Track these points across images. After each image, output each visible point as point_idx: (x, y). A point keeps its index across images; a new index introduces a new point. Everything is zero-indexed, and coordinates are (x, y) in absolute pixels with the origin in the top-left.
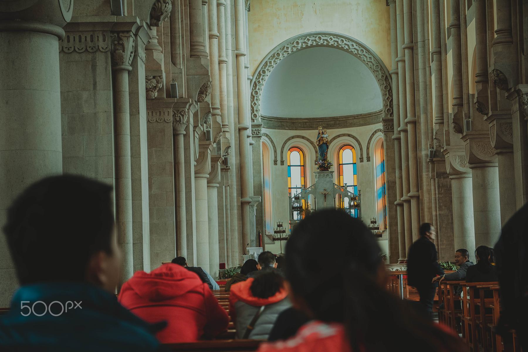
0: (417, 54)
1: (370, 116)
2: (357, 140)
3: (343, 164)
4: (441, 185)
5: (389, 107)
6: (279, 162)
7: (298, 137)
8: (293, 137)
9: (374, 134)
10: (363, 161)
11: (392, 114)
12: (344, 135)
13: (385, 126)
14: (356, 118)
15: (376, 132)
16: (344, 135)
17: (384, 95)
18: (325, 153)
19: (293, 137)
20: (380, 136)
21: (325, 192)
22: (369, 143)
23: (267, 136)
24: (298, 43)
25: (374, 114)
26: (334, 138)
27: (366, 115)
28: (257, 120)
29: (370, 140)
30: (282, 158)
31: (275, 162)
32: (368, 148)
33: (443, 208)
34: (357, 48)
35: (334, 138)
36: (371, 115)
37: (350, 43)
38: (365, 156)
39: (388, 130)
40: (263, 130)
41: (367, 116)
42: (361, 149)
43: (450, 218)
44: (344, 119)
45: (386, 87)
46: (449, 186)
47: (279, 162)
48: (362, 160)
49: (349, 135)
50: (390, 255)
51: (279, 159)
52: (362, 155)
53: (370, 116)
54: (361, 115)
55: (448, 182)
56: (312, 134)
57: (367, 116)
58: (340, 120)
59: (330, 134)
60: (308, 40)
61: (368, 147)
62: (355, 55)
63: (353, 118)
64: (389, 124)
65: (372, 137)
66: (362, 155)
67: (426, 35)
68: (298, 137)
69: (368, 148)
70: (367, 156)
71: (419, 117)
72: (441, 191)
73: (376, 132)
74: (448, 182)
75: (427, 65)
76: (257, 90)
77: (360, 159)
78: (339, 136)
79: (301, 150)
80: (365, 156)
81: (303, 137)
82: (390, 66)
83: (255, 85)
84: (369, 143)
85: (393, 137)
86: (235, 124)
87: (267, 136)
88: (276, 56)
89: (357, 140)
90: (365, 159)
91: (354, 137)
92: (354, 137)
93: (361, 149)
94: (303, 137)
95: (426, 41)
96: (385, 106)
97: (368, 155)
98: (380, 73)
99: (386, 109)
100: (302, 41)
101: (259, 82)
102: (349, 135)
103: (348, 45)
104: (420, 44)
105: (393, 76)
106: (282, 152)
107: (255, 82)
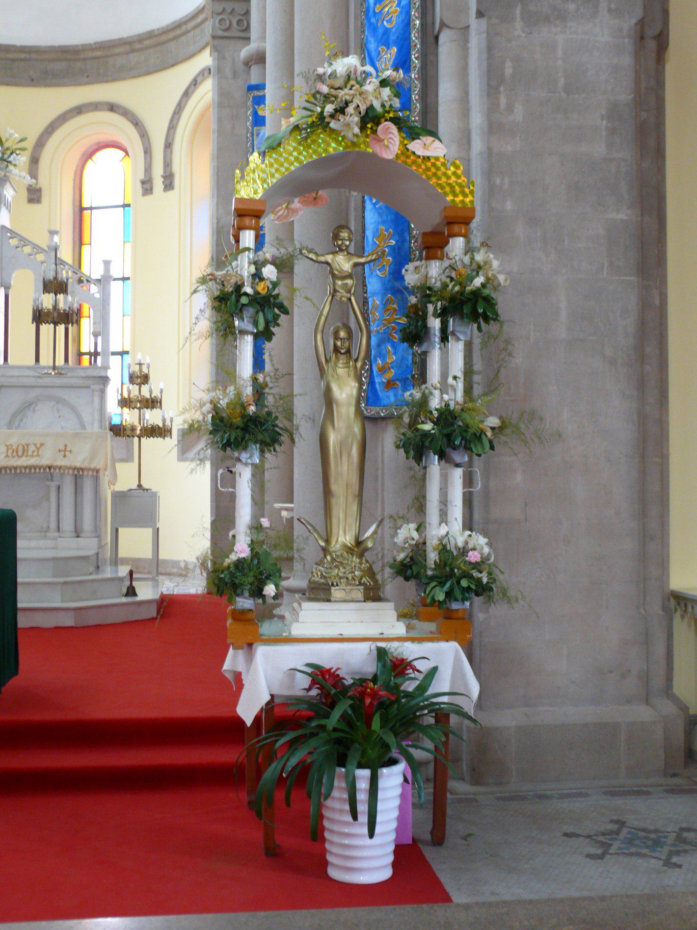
1: (178, 32)
2: (137, 123)
4: (508, 70)
9: (190, 91)
10: (152, 189)
12: (95, 106)
13: (219, 14)
14: (137, 46)
15: (195, 83)
16: (95, 106)
22: (172, 127)
25: (193, 23)
27: (166, 31)
29: (177, 117)
32: (168, 145)
33: (520, 230)
36: (184, 28)
39: (226, 34)
41: (171, 35)
42: (148, 151)
43: (563, 305)
44: (99, 53)
46: (562, 81)
48: (147, 186)
49: (112, 108)
50: (213, 519)
52: (148, 169)
53: (178, 32)
54: (150, 35)
55: (560, 53)
57: (171, 35)
58: (84, 59)
61: (170, 141)
63: (128, 48)
64: (233, 10)
65: (182, 106)
66: (148, 169)
69: (168, 145)
70: (165, 171)
72: (510, 108)
73: (195, 83)
74: (560, 53)
77: (143, 182)
78: (79, 110)
84: (172, 127)
89: (137, 123)
90: (158, 183)
91: (126, 113)
92: (126, 113)
93: (148, 151)
97: (168, 169)
102: (112, 108)
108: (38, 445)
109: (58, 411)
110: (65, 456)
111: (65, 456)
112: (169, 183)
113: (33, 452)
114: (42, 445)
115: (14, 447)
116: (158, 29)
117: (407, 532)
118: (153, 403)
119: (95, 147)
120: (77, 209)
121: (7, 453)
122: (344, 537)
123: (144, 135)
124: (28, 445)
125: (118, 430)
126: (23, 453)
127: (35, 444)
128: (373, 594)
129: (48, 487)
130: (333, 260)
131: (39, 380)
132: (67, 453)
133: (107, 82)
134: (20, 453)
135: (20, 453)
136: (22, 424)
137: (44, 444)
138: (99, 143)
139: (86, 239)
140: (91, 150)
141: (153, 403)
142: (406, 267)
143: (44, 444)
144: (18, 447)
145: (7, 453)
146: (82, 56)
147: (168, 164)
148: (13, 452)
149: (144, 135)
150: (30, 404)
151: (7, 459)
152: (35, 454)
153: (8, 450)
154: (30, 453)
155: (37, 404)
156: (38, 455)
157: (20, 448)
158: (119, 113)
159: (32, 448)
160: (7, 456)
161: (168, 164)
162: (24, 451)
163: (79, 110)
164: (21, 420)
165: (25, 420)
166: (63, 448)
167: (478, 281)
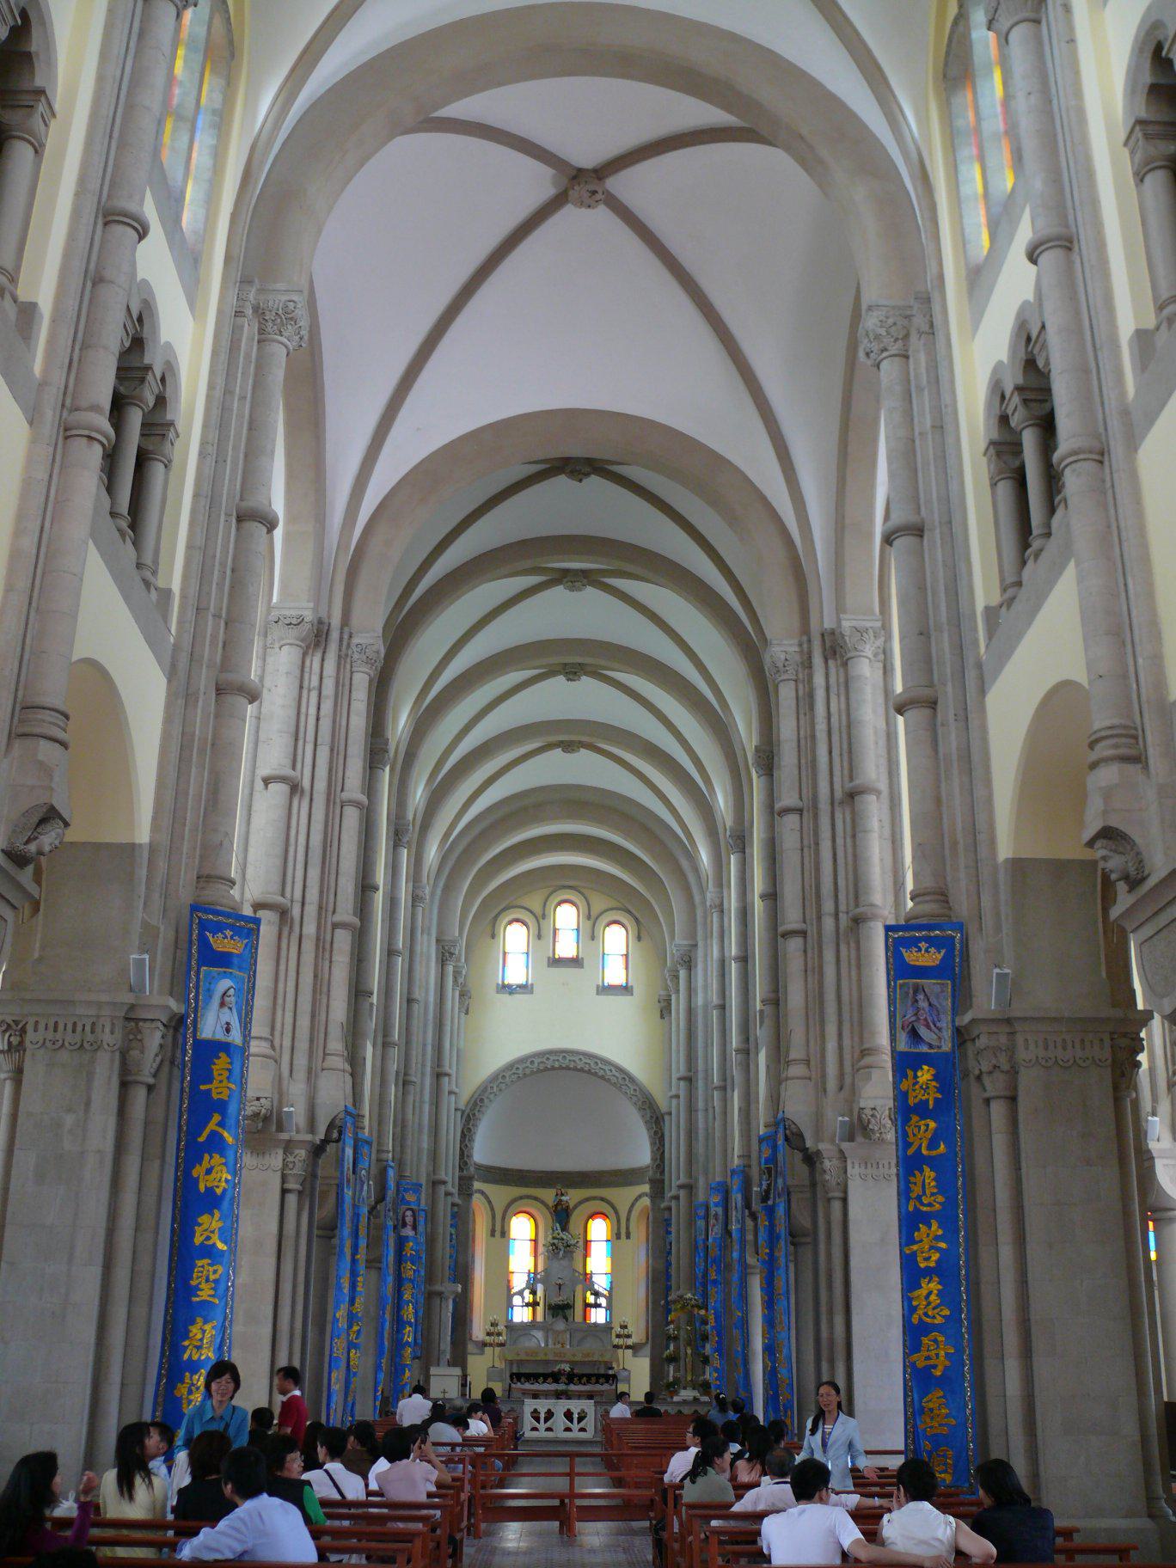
0: (697, 1088)
2: (613, 1207)
5: (658, 1162)
6: (498, 1234)
7: (528, 1197)
8: (521, 1198)
11: (663, 1172)
12: (595, 1198)
15: (640, 1197)
16: (595, 1198)
17: (653, 1144)
19: (521, 1198)
20: (646, 1201)
21: (560, 1281)
22: (630, 1211)
23: (482, 1193)
24: (532, 1062)
26: (580, 1203)
28: (468, 1169)
30: (503, 1227)
31: (493, 1234)
32: (628, 1220)
34: (617, 1074)
35: (580, 1203)
37: (606, 1068)
38: (623, 1231)
40: (477, 1185)
42: (618, 1221)
45: (656, 1133)
47: (498, 1234)
48: (618, 1236)
49: (602, 1199)
51: (498, 1228)
52: (619, 1229)
54: (620, 1171)
56: (549, 1195)
59: (572, 1196)
60: (548, 1059)
62: (614, 1084)
66: (619, 1229)
67: (710, 1062)
68: (528, 1197)
69: (628, 1220)
71: (697, 1180)
73: (640, 1197)
75: (710, 1105)
76: (470, 1126)
78: (587, 1200)
79: (532, 1216)
80: (623, 1231)
81: (536, 1199)
82: (662, 1103)
83: (468, 1119)
84: (630, 1211)
85: (662, 1206)
86: (428, 1175)
87: (482, 1193)
88: (500, 1080)
89: (613, 1207)
91: (608, 1202)
92: (608, 1202)
93: (618, 1221)
94: (536, 1199)
95: (710, 1071)
96: (654, 1159)
98: (648, 1111)
100: (540, 1060)
101: (474, 1115)
102: (602, 1199)
103: (604, 1070)
104: (701, 1075)
105: (666, 1117)
106: (503, 1218)
107: (469, 1115)
112: (628, 1237)
117: (702, 1378)
118: (629, 1336)
122: (689, 1378)
123: (617, 1213)
125: (617, 1347)
128: (694, 1389)
141: (629, 1336)
147: (628, 1228)
149: (617, 1213)
161: (628, 1228)
163: (587, 1200)
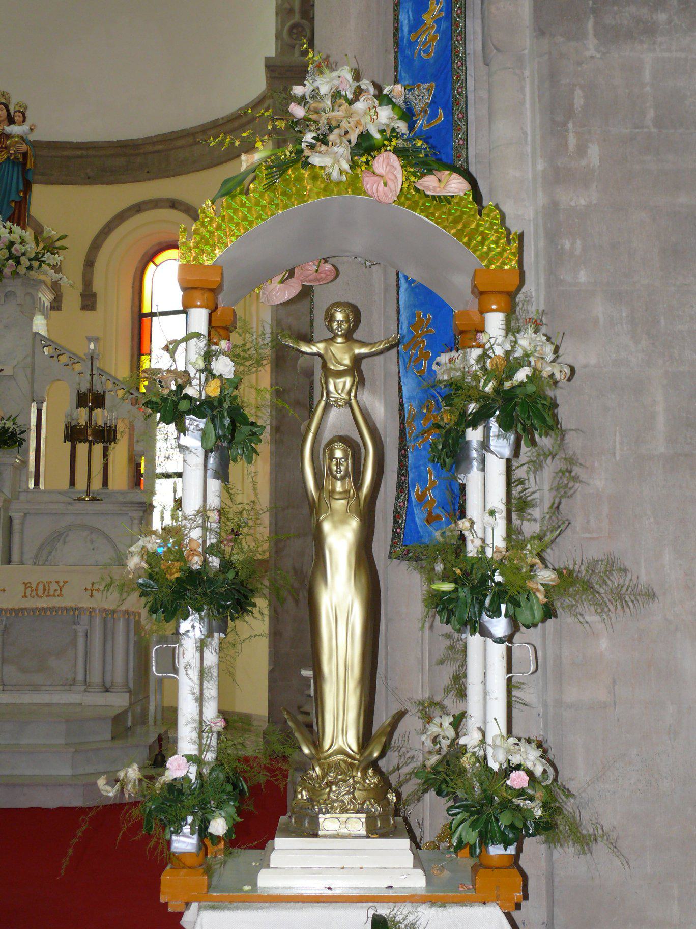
3: (152, 315)
4: (579, 100)
5: (297, 18)
12: (155, 204)
16: (155, 204)
18: (13, 205)
33: (600, 309)
43: (660, 408)
44: (160, 147)
46: (651, 114)
50: (271, 667)
55: (647, 76)
58: (145, 154)
63: (191, 140)
72: (582, 150)
74: (647, 76)
78: (138, 208)
99: (283, 24)
102: (173, 204)
108: (61, 584)
109: (92, 542)
110: (91, 596)
111: (91, 596)
113: (55, 591)
114: (65, 583)
115: (34, 586)
116: (222, 118)
119: (157, 248)
120: (136, 316)
121: (25, 593)
124: (49, 583)
126: (44, 594)
127: (57, 582)
129: (76, 631)
130: (326, 349)
131: (70, 507)
132: (94, 593)
133: (168, 177)
134: (40, 592)
135: (40, 592)
136: (50, 557)
137: (67, 582)
138: (160, 244)
139: (145, 349)
140: (151, 251)
142: (438, 359)
143: (67, 582)
144: (38, 585)
145: (25, 593)
146: (142, 151)
148: (32, 591)
150: (60, 535)
151: (25, 599)
152: (57, 593)
153: (26, 588)
154: (52, 593)
155: (67, 536)
156: (60, 595)
157: (41, 587)
158: (180, 210)
159: (54, 586)
160: (25, 596)
162: (44, 589)
163: (138, 208)
164: (50, 553)
165: (53, 554)
166: (89, 587)
167: (522, 375)
